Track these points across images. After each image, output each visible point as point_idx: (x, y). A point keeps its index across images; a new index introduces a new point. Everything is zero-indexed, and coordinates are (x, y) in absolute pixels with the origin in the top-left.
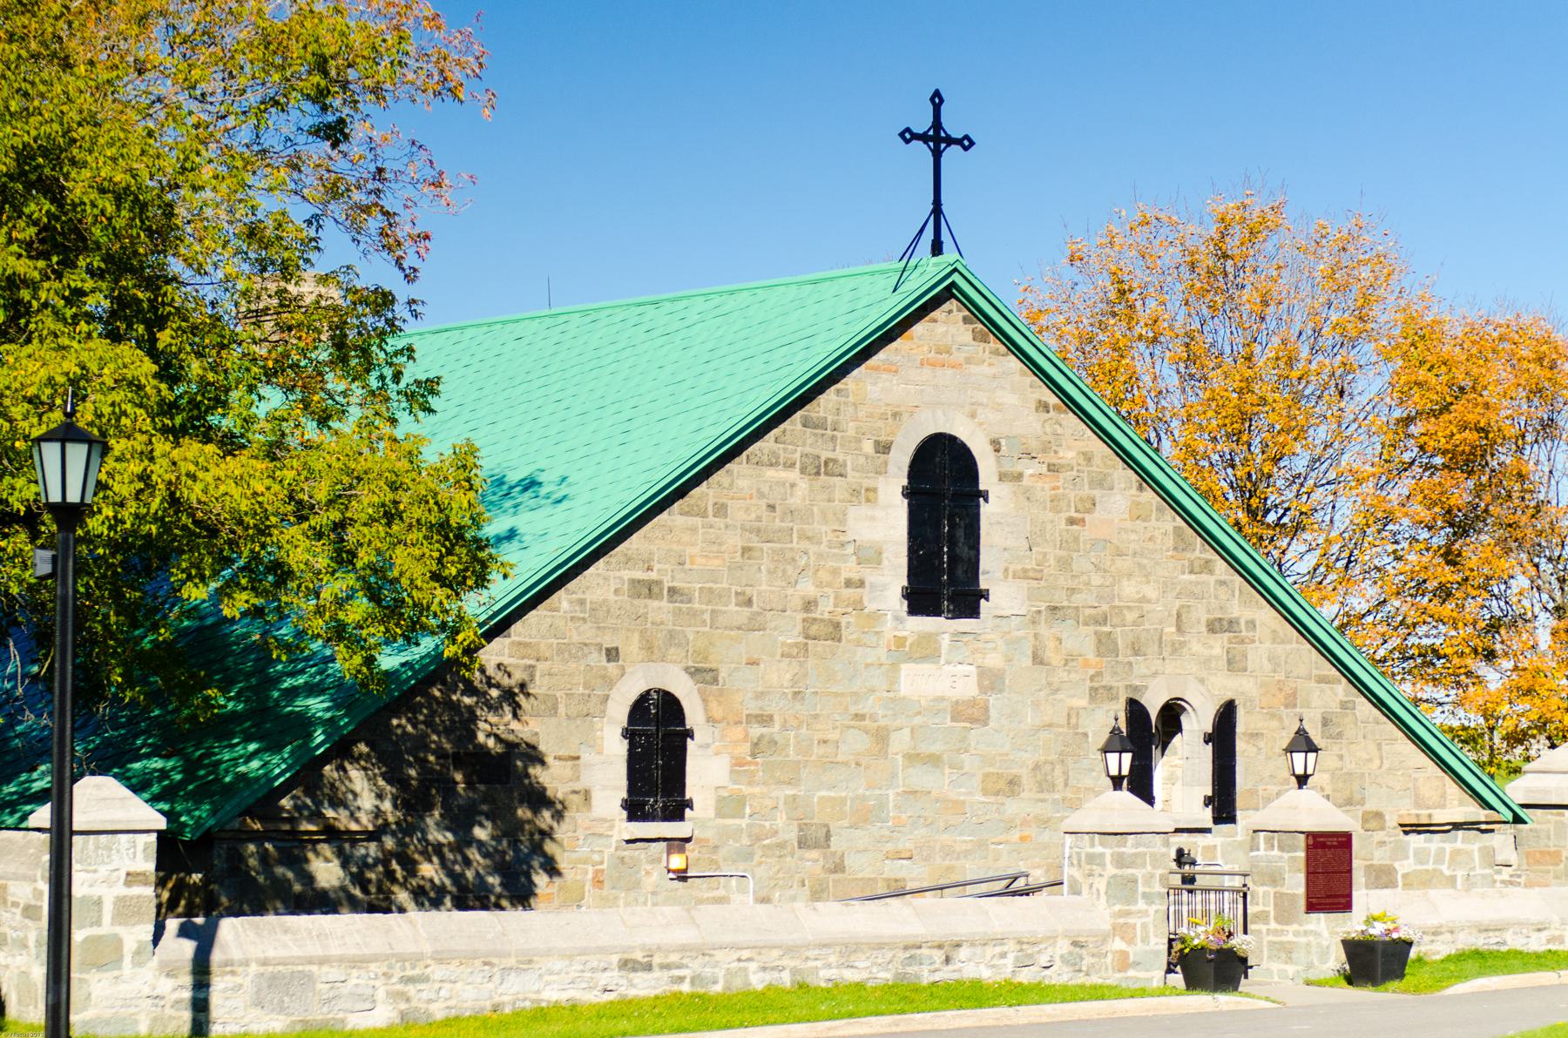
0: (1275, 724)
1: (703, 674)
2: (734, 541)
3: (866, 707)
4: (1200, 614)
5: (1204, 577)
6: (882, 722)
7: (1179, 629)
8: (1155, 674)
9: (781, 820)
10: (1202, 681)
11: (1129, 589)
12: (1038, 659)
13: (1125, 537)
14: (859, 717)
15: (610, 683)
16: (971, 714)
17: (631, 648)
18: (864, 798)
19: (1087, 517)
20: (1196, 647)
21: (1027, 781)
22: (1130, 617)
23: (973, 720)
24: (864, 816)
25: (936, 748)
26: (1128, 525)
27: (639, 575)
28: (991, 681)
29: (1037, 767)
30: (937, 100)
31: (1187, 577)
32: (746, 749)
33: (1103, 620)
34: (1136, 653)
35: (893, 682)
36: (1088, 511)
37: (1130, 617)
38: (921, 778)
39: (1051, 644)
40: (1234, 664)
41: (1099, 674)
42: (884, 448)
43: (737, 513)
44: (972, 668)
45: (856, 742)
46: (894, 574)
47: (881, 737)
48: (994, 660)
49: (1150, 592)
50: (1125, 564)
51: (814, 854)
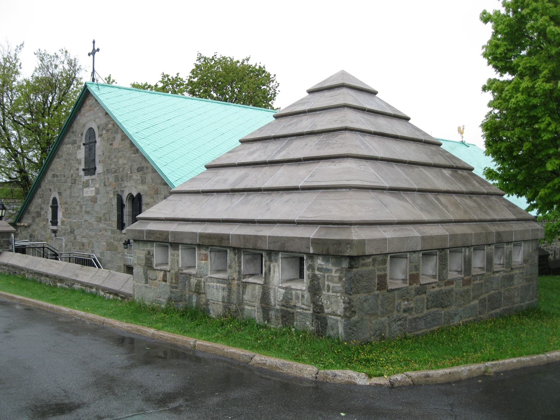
0: (152, 200)
1: (60, 194)
2: (63, 163)
3: (79, 200)
4: (135, 167)
5: (137, 154)
6: (82, 203)
7: (131, 173)
8: (126, 187)
9: (68, 226)
10: (136, 187)
11: (121, 162)
12: (105, 185)
13: (120, 146)
14: (78, 202)
15: (50, 196)
16: (94, 200)
17: (52, 189)
18: (79, 222)
19: (114, 143)
20: (134, 177)
21: (103, 218)
22: (121, 169)
23: (94, 202)
24: (79, 227)
25: (88, 210)
26: (121, 143)
27: (53, 173)
28: (98, 191)
29: (104, 215)
30: (94, 42)
31: (133, 155)
32: (64, 210)
33: (116, 172)
34: (122, 180)
35: (83, 193)
36: (113, 141)
37: (121, 169)
38: (87, 217)
39: (107, 180)
40: (143, 182)
41: (115, 187)
42: (82, 135)
43: (64, 157)
44: (94, 188)
45: (78, 208)
46: (83, 166)
47: (81, 207)
48: (97, 186)
49: (125, 162)
50: (120, 154)
51: (72, 235)
